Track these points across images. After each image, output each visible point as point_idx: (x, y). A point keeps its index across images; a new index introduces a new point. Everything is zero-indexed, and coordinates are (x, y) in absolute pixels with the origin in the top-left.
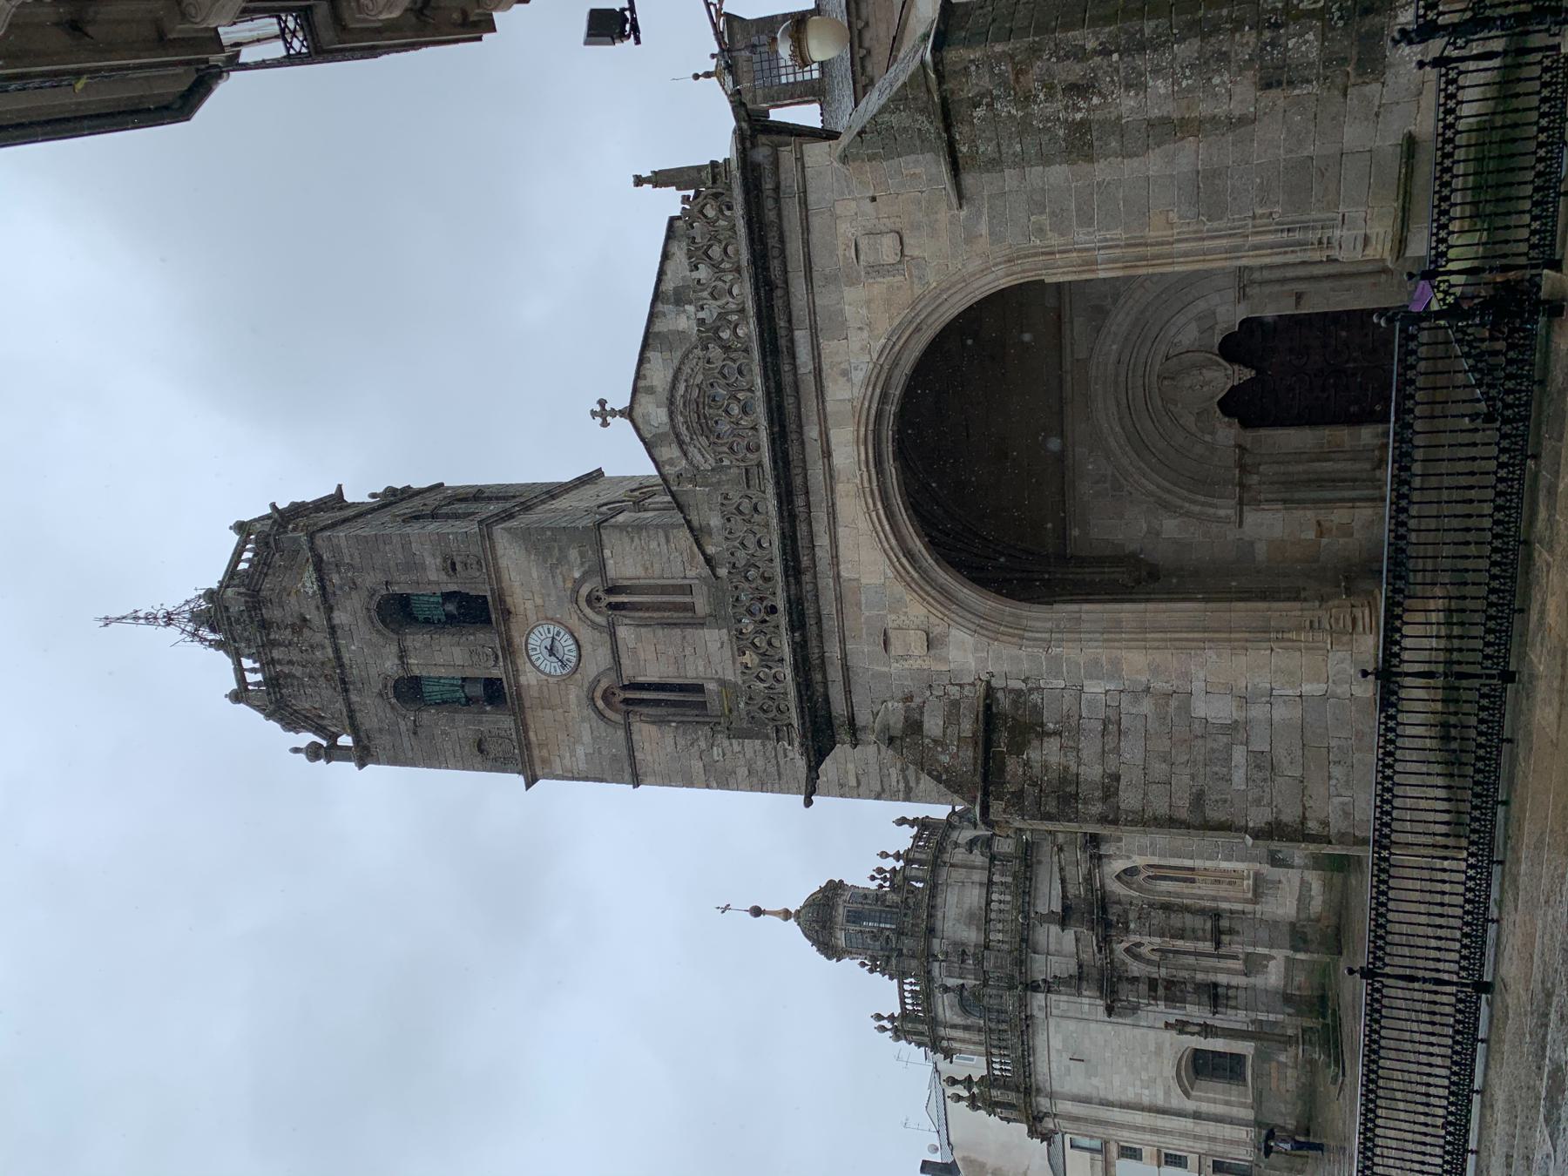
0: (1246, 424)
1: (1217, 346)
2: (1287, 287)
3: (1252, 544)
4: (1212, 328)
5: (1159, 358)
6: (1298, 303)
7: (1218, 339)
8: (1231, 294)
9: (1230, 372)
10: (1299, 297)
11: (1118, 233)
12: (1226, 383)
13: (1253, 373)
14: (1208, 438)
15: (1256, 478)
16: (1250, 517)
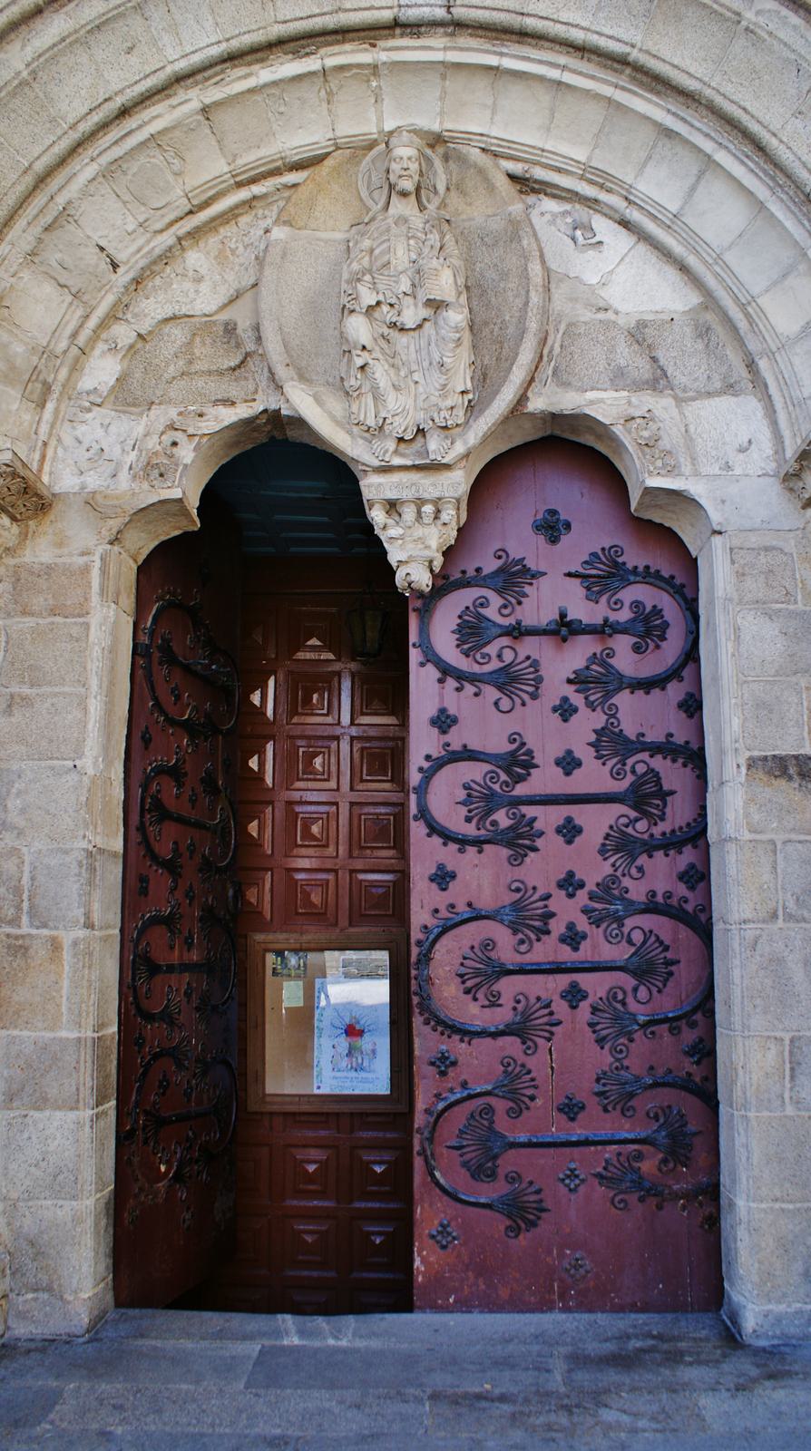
4: (658, 380)
14: (102, 371)
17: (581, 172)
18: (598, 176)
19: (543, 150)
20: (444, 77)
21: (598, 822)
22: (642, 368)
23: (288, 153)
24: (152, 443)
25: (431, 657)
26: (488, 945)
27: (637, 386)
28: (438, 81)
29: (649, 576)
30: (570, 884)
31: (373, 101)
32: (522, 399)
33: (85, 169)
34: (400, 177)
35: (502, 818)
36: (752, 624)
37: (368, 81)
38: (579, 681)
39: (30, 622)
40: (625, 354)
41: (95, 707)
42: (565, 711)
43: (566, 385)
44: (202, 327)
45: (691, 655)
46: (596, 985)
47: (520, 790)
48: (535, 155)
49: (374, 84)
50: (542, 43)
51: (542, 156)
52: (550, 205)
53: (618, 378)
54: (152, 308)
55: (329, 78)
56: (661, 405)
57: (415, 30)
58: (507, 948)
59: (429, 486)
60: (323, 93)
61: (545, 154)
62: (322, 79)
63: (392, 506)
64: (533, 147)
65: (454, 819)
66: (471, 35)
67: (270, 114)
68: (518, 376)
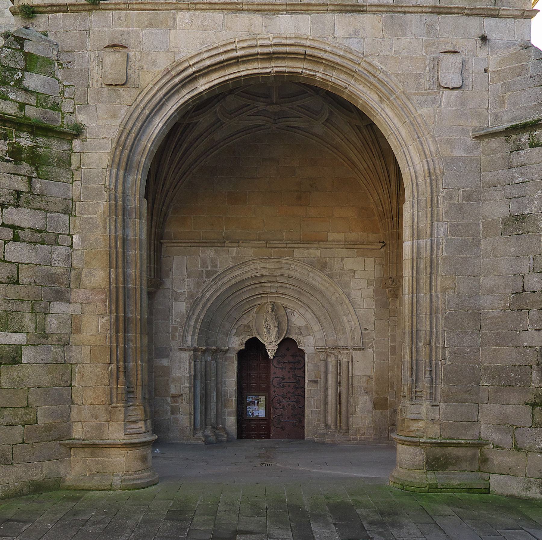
0: (241, 354)
1: (290, 337)
2: (322, 376)
3: (168, 356)
4: (301, 334)
5: (285, 303)
6: (311, 381)
7: (294, 337)
8: (321, 344)
9: (274, 344)
10: (316, 382)
11: (442, 253)
12: (267, 342)
13: (272, 357)
14: (234, 332)
15: (209, 359)
16: (186, 356)
21: (292, 385)
22: (299, 333)
24: (240, 341)
25: (273, 365)
26: (279, 399)
27: (298, 335)
29: (300, 356)
30: (289, 392)
32: (285, 336)
33: (233, 310)
35: (281, 385)
36: (309, 364)
38: (291, 368)
39: (227, 363)
40: (297, 331)
41: (236, 373)
42: (289, 372)
43: (290, 335)
44: (246, 325)
45: (304, 365)
46: (292, 404)
47: (283, 381)
52: (289, 310)
53: (296, 334)
54: (240, 323)
56: (301, 337)
58: (281, 400)
59: (274, 348)
63: (269, 350)
65: (276, 385)
68: (284, 335)
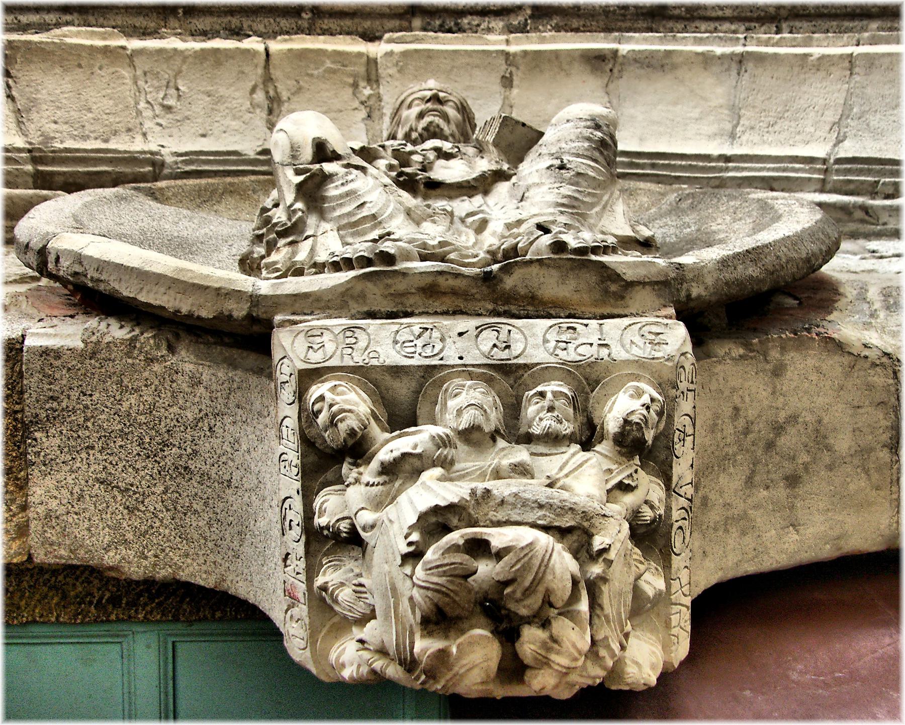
17: (822, 177)
18: (860, 172)
19: (727, 159)
20: (507, 82)
23: (169, 159)
28: (497, 87)
31: (363, 114)
34: (421, 116)
37: (355, 86)
48: (721, 170)
49: (367, 91)
50: (697, 23)
51: (727, 169)
55: (276, 73)
57: (450, 23)
60: (260, 96)
61: (730, 164)
62: (260, 71)
64: (707, 158)
66: (558, 29)
67: (142, 105)
